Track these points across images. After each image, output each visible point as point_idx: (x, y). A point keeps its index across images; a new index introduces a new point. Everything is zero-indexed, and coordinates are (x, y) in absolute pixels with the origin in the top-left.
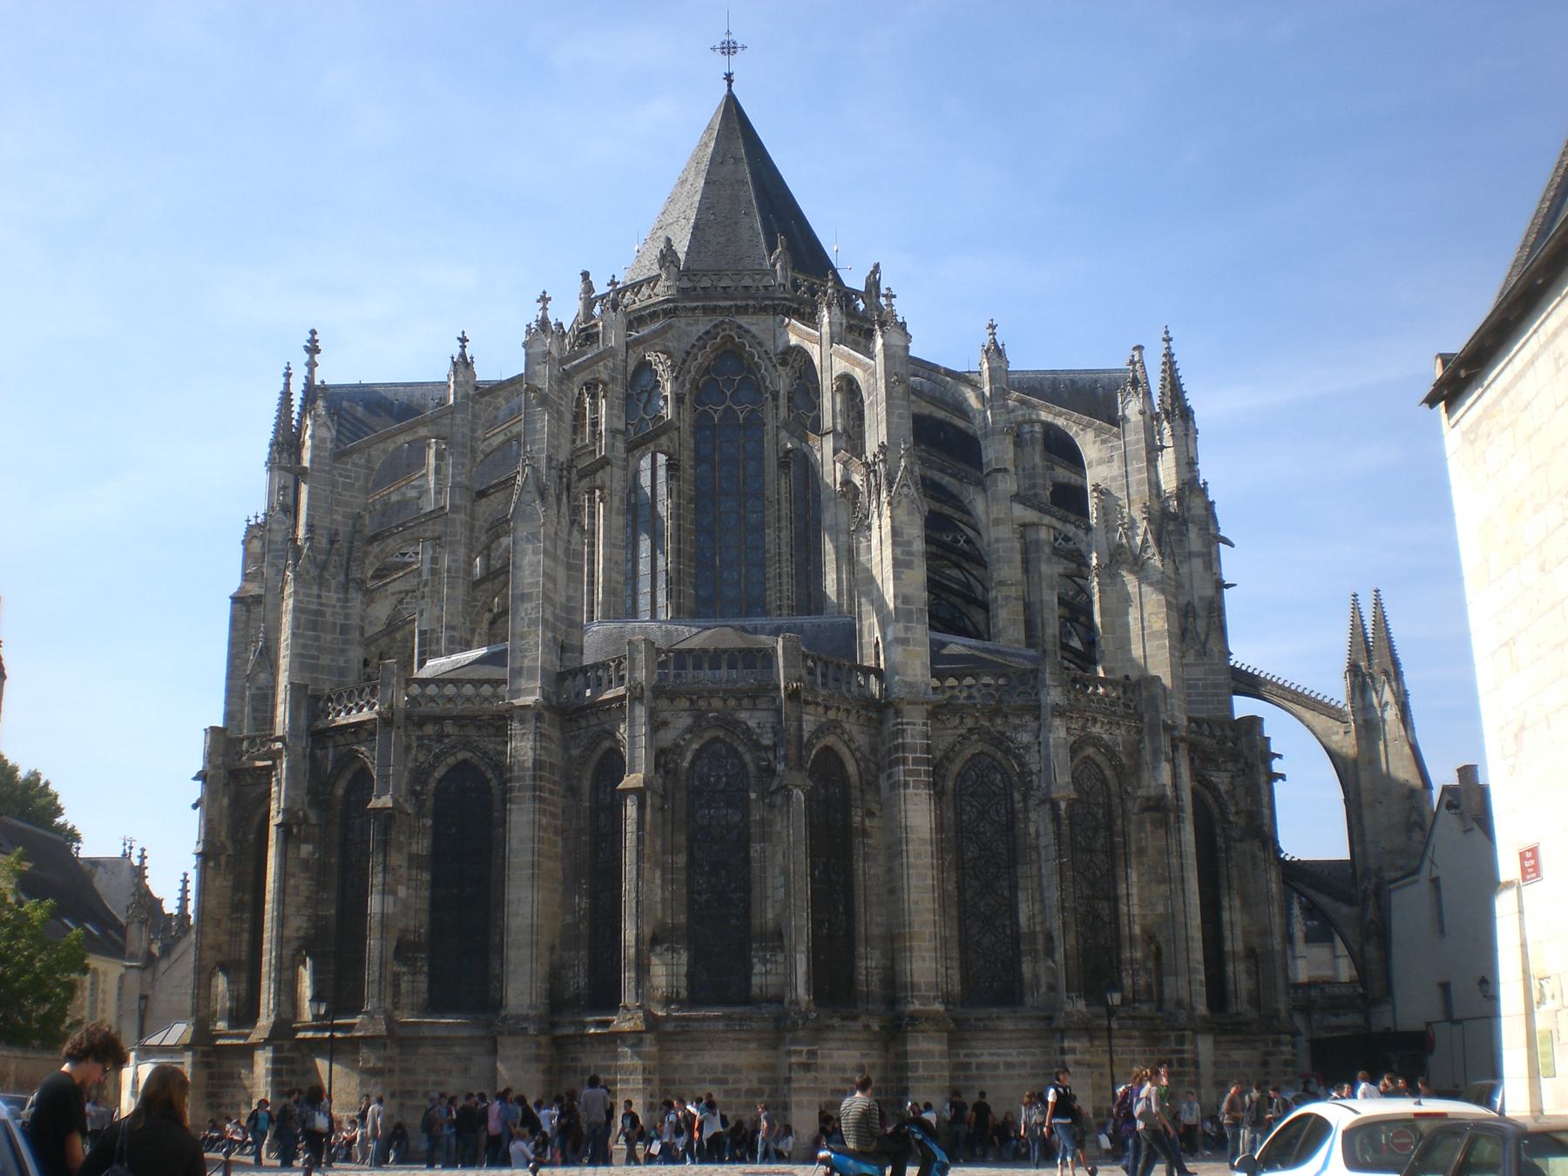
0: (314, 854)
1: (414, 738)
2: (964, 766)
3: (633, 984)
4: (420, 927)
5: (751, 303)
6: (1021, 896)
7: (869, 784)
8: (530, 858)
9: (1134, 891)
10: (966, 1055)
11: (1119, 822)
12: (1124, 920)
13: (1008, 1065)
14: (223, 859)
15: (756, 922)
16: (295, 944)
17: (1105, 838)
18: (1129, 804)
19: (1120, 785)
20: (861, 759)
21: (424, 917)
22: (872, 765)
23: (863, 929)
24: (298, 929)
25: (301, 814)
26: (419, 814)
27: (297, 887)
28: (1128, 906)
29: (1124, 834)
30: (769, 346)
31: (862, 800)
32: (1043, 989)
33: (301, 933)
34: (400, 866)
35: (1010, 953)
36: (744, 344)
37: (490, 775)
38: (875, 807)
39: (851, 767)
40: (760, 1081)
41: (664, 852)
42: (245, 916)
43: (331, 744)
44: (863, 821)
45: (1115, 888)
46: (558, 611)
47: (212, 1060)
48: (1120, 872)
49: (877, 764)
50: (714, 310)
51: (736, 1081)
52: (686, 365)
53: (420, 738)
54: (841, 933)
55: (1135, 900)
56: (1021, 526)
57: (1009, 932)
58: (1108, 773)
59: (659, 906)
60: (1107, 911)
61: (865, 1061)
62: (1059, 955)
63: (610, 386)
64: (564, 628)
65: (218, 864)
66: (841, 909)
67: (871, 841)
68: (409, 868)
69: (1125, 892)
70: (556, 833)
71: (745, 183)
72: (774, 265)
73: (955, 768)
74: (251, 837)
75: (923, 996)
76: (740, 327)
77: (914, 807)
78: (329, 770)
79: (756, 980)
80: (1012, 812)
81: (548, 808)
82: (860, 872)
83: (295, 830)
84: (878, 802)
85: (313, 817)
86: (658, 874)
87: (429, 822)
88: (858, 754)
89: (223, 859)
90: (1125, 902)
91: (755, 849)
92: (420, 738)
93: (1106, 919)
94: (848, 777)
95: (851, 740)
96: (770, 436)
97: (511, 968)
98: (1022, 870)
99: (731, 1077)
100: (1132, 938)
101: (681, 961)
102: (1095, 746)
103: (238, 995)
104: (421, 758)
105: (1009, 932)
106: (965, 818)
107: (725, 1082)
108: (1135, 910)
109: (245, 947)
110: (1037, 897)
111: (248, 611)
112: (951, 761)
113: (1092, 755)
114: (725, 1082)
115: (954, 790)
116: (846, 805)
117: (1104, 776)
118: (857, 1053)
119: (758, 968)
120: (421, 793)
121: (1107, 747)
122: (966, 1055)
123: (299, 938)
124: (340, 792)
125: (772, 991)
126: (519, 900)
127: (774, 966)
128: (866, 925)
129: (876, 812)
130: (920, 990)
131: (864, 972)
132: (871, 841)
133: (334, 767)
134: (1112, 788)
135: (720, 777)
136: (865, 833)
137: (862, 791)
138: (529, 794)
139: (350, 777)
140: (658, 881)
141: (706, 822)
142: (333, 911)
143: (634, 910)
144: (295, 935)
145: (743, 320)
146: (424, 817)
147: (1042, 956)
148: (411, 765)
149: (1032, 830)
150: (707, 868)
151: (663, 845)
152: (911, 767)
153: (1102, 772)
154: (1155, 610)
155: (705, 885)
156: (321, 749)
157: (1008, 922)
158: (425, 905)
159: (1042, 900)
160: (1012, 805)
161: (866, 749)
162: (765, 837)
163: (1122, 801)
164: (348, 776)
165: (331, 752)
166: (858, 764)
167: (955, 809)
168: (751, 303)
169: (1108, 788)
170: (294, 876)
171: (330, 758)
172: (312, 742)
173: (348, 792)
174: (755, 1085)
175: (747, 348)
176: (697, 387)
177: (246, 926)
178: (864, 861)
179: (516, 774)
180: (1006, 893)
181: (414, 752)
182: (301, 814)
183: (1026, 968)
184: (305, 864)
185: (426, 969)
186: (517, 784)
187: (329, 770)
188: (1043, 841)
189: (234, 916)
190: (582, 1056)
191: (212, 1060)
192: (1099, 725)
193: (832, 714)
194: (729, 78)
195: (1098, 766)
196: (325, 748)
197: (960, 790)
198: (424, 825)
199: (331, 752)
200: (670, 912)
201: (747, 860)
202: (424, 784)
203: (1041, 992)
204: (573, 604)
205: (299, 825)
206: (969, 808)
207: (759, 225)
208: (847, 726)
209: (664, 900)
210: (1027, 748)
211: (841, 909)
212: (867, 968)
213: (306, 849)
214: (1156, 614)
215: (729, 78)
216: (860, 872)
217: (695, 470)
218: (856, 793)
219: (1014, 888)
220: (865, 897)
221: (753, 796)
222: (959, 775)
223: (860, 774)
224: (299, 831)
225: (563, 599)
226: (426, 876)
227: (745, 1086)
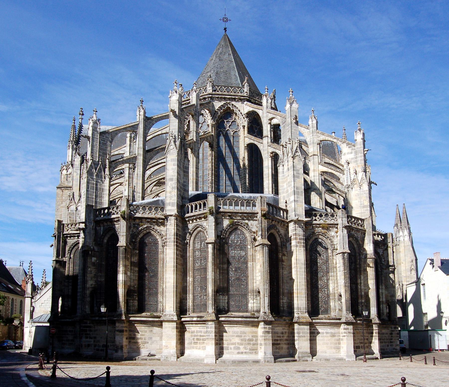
0: (97, 261)
1: (132, 224)
2: (312, 242)
3: (211, 305)
4: (135, 285)
5: (237, 97)
6: (330, 282)
7: (284, 245)
8: (173, 264)
9: (362, 282)
10: (313, 330)
11: (358, 261)
12: (359, 290)
13: (327, 333)
15: (250, 287)
16: (90, 289)
17: (354, 265)
18: (361, 256)
19: (359, 250)
20: (282, 238)
21: (136, 282)
22: (285, 240)
23: (282, 290)
24: (91, 285)
25: (92, 247)
26: (134, 249)
27: (91, 271)
28: (361, 286)
29: (360, 265)
30: (242, 111)
31: (282, 251)
32: (337, 310)
33: (93, 286)
34: (128, 265)
35: (327, 299)
36: (234, 110)
38: (285, 253)
39: (279, 240)
40: (252, 336)
41: (220, 264)
43: (102, 225)
44: (282, 257)
45: (357, 280)
46: (181, 185)
48: (358, 276)
49: (286, 240)
50: (225, 99)
51: (244, 336)
52: (215, 115)
53: (134, 224)
54: (275, 291)
55: (362, 284)
56: (321, 172)
57: (326, 293)
58: (355, 246)
59: (218, 281)
60: (354, 288)
61: (284, 331)
62: (343, 300)
63: (194, 116)
64: (183, 191)
66: (275, 284)
67: (284, 264)
68: (131, 266)
69: (360, 282)
70: (181, 257)
71: (232, 62)
72: (244, 86)
73: (310, 242)
75: (302, 311)
76: (233, 105)
77: (299, 253)
79: (250, 305)
80: (327, 257)
81: (179, 248)
82: (281, 273)
83: (90, 253)
84: (286, 252)
85: (96, 249)
86: (218, 270)
87: (138, 252)
88: (281, 236)
90: (360, 285)
91: (250, 264)
92: (134, 224)
93: (354, 290)
94: (277, 243)
95: (279, 231)
96: (242, 140)
98: (330, 274)
99: (243, 335)
100: (361, 295)
101: (225, 298)
102: (352, 237)
104: (135, 231)
105: (326, 293)
106: (313, 258)
107: (241, 336)
108: (363, 287)
110: (336, 282)
111: (62, 192)
112: (309, 240)
113: (351, 240)
114: (241, 336)
115: (310, 249)
116: (277, 252)
117: (354, 247)
118: (281, 328)
119: (251, 301)
120: (135, 242)
121: (355, 238)
122: (313, 330)
123: (92, 288)
124: (105, 241)
125: (255, 309)
127: (256, 301)
128: (283, 289)
129: (286, 255)
130: (301, 309)
131: (282, 303)
132: (284, 264)
133: (103, 233)
134: (357, 251)
135: (238, 241)
136: (283, 261)
137: (282, 248)
138: (173, 244)
140: (218, 273)
141: (233, 255)
143: (211, 282)
144: (91, 286)
145: (233, 103)
146: (136, 250)
147: (337, 300)
148: (131, 233)
149: (334, 262)
150: (234, 270)
151: (220, 261)
152: (299, 241)
153: (354, 246)
154: (365, 199)
155: (233, 275)
156: (99, 227)
157: (326, 290)
158: (137, 279)
159: (337, 283)
160: (328, 255)
161: (283, 235)
162: (253, 260)
163: (360, 255)
164: (108, 236)
166: (281, 239)
167: (310, 254)
168: (237, 97)
169: (355, 251)
170: (90, 267)
171: (102, 230)
172: (96, 224)
174: (251, 338)
175: (235, 112)
176: (218, 123)
178: (282, 269)
179: (168, 237)
180: (326, 281)
181: (132, 228)
182: (92, 247)
183: (332, 304)
184: (94, 264)
185: (137, 299)
186: (168, 240)
188: (338, 266)
192: (354, 231)
193: (273, 222)
195: (352, 244)
196: (100, 226)
197: (312, 249)
198: (136, 252)
199: (102, 228)
200: (222, 283)
201: (247, 267)
202: (136, 239)
203: (336, 311)
204: (185, 184)
205: (91, 251)
206: (314, 255)
207: (237, 74)
208: (278, 227)
209: (220, 279)
210: (333, 237)
211: (275, 284)
212: (283, 302)
213: (94, 259)
214: (366, 200)
216: (281, 273)
217: (218, 148)
218: (280, 248)
219: (328, 280)
220: (282, 280)
221: (249, 247)
222: (311, 244)
223: (281, 242)
224: (91, 253)
225: (182, 182)
226: (137, 269)
227: (247, 338)
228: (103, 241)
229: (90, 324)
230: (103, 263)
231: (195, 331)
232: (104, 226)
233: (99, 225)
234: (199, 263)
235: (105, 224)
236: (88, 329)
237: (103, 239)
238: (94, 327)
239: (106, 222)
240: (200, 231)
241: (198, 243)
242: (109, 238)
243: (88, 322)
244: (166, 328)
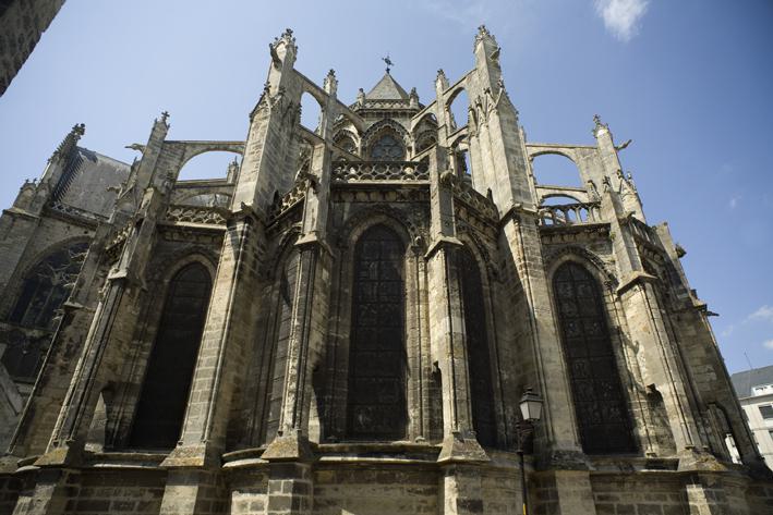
14: (138, 291)
37: (479, 258)
42: (147, 344)
47: (78, 486)
65: (133, 293)
74: (166, 281)
78: (345, 218)
89: (138, 291)
97: (554, 407)
103: (123, 417)
109: (141, 372)
126: (550, 350)
139: (366, 228)
142: (347, 336)
156: (335, 202)
164: (365, 227)
165: (347, 207)
173: (361, 238)
177: (146, 353)
187: (345, 218)
189: (135, 342)
190: (619, 494)
191: (78, 486)
194: (388, 70)
196: (341, 201)
199: (347, 207)
215: (388, 70)
228: (348, 236)
229: (306, 476)
230: (347, 291)
231: (636, 507)
232: (355, 201)
233: (340, 198)
234: (577, 330)
235: (362, 196)
236: (301, 496)
237: (350, 230)
238: (317, 491)
239: (368, 193)
240: (569, 263)
241: (565, 286)
242: (364, 233)
243: (304, 471)
244: (567, 494)
